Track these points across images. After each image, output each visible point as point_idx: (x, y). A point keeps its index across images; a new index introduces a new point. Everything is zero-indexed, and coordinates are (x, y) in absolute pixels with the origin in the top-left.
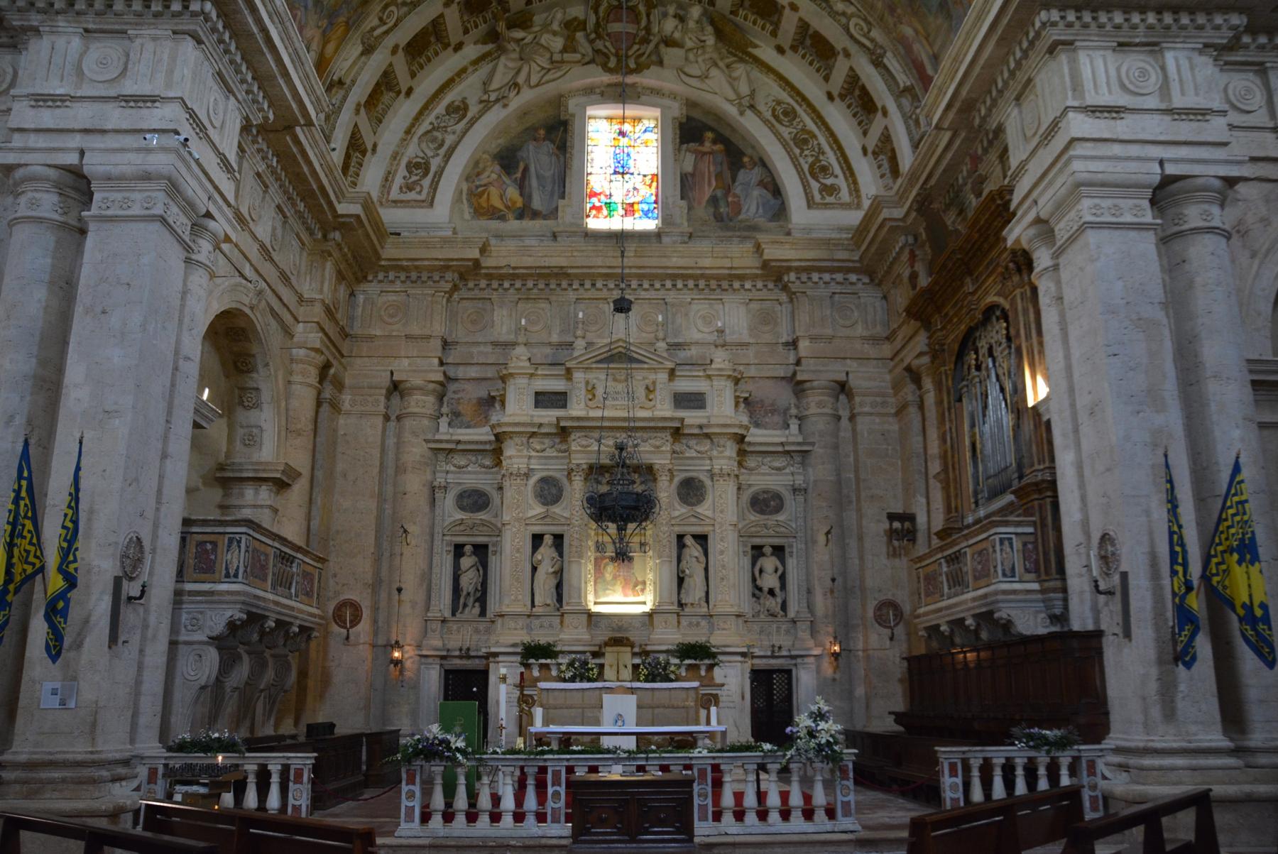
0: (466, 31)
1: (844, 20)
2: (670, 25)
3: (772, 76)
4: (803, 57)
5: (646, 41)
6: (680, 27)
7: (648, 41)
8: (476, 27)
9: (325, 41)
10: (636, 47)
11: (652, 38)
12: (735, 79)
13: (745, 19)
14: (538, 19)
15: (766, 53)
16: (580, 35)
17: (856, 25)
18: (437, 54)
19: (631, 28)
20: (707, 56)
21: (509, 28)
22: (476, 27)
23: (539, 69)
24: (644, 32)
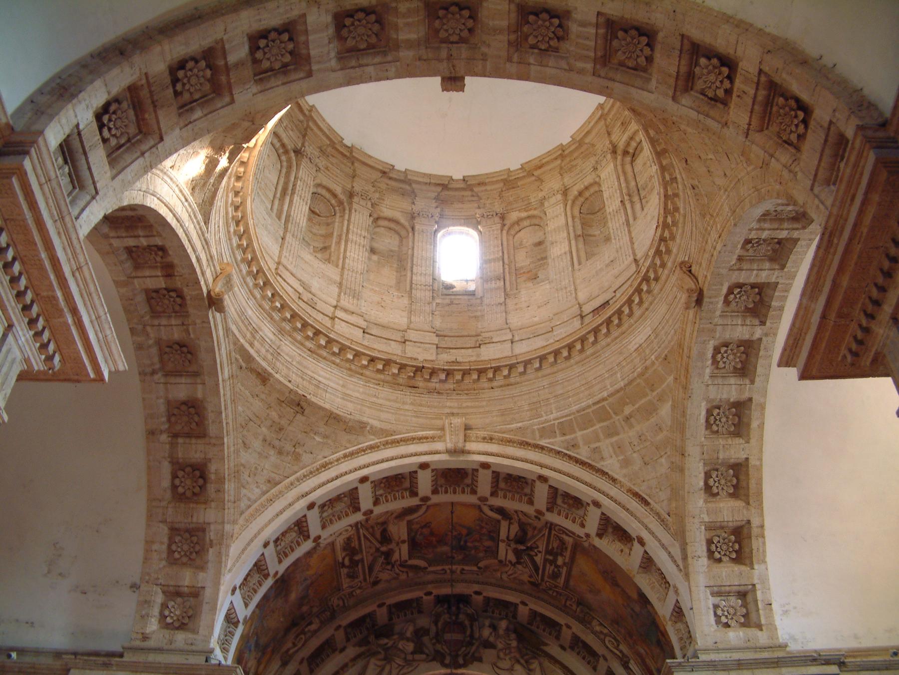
0: (348, 640)
1: (602, 637)
2: (486, 632)
3: (557, 665)
4: (578, 654)
5: (470, 644)
6: (493, 634)
7: (472, 644)
8: (355, 636)
9: (259, 662)
10: (464, 649)
11: (474, 641)
12: (530, 670)
13: (538, 627)
14: (397, 628)
15: (554, 649)
16: (426, 639)
17: (609, 641)
18: (328, 656)
19: (459, 637)
20: (513, 655)
21: (378, 637)
22: (355, 636)
23: (397, 666)
24: (468, 639)
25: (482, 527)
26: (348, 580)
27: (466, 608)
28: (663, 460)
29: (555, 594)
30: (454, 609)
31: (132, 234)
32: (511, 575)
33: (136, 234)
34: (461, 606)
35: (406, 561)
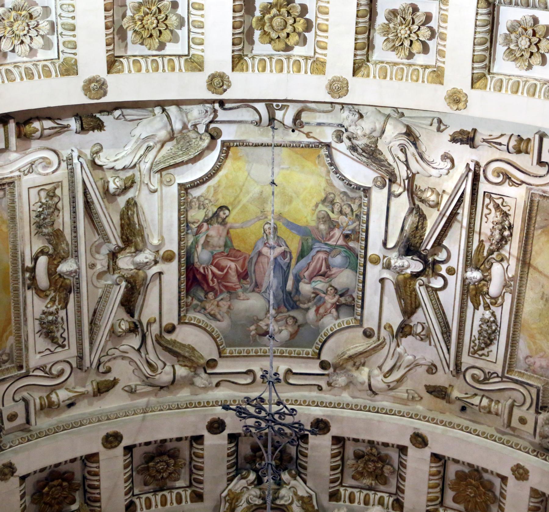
25: (333, 225)
26: (42, 344)
27: (293, 482)
29: (485, 402)
30: (268, 481)
32: (391, 371)
34: (285, 476)
35: (171, 329)
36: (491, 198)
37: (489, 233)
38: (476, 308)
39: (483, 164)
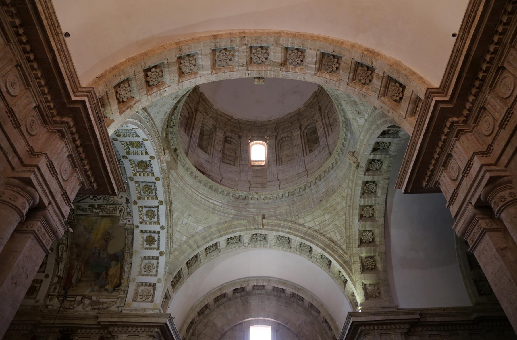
28: (185, 237)
31: (317, 62)
33: (317, 64)
36: (115, 208)
37: (107, 208)
38: (88, 206)
39: (122, 205)
